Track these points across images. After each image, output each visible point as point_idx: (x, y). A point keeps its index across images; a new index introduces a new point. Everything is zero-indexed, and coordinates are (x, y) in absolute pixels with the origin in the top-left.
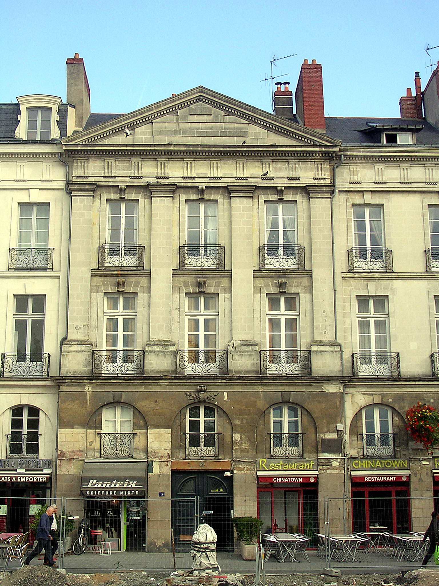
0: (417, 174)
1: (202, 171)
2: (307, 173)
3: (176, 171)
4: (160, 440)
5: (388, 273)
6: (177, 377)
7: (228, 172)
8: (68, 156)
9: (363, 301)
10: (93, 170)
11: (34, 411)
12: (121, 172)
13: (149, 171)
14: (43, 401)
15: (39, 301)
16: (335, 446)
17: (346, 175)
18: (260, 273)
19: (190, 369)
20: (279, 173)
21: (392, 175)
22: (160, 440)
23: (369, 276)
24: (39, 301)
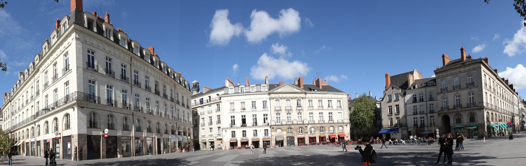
0: (317, 95)
1: (288, 95)
2: (303, 95)
3: (284, 95)
4: (285, 133)
5: (313, 109)
6: (287, 125)
7: (292, 95)
8: (269, 94)
9: (310, 113)
10: (273, 96)
11: (267, 130)
12: (277, 96)
13: (281, 95)
14: (269, 128)
15: (267, 115)
16: (307, 133)
17: (308, 95)
18: (297, 110)
19: (288, 123)
20: (298, 95)
21: (313, 96)
22: (285, 133)
23: (311, 110)
24: (267, 115)
